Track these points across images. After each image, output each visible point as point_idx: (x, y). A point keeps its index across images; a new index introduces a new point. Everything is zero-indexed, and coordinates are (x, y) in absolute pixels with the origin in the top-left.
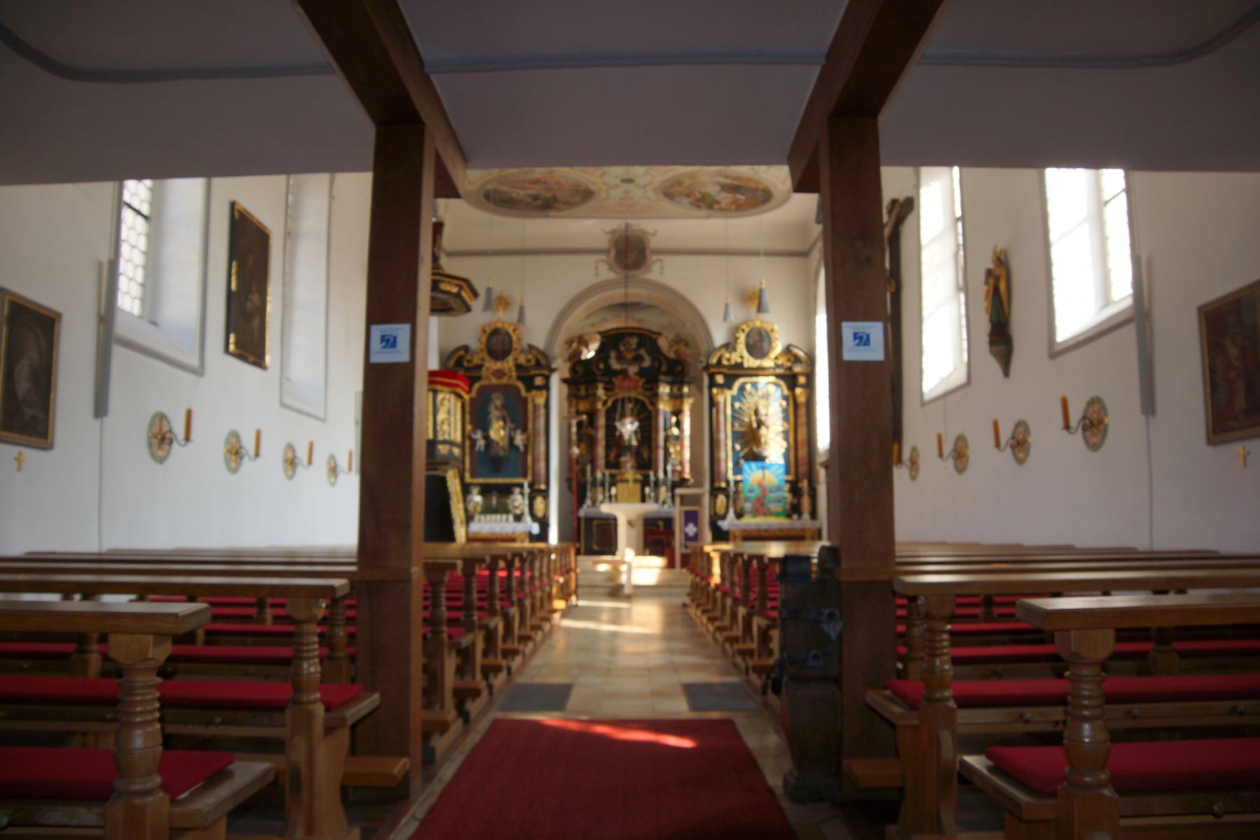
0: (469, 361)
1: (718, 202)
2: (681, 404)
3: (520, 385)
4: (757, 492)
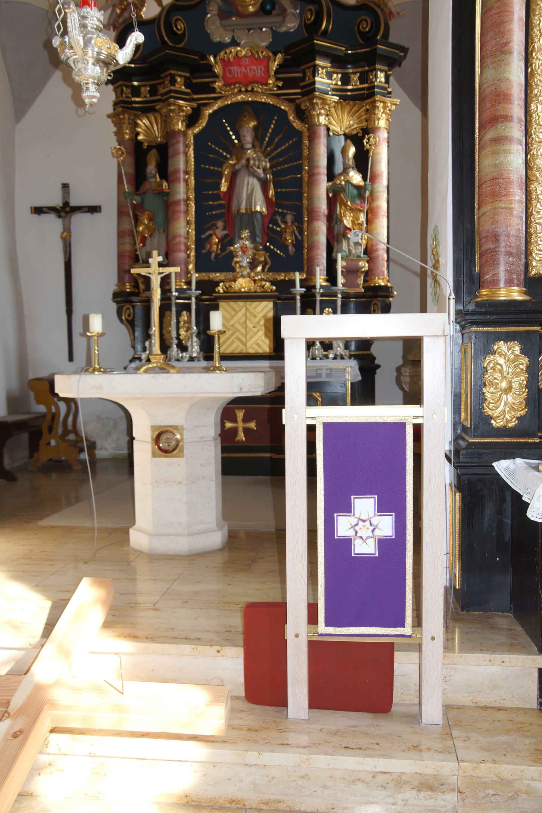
2: (371, 112)
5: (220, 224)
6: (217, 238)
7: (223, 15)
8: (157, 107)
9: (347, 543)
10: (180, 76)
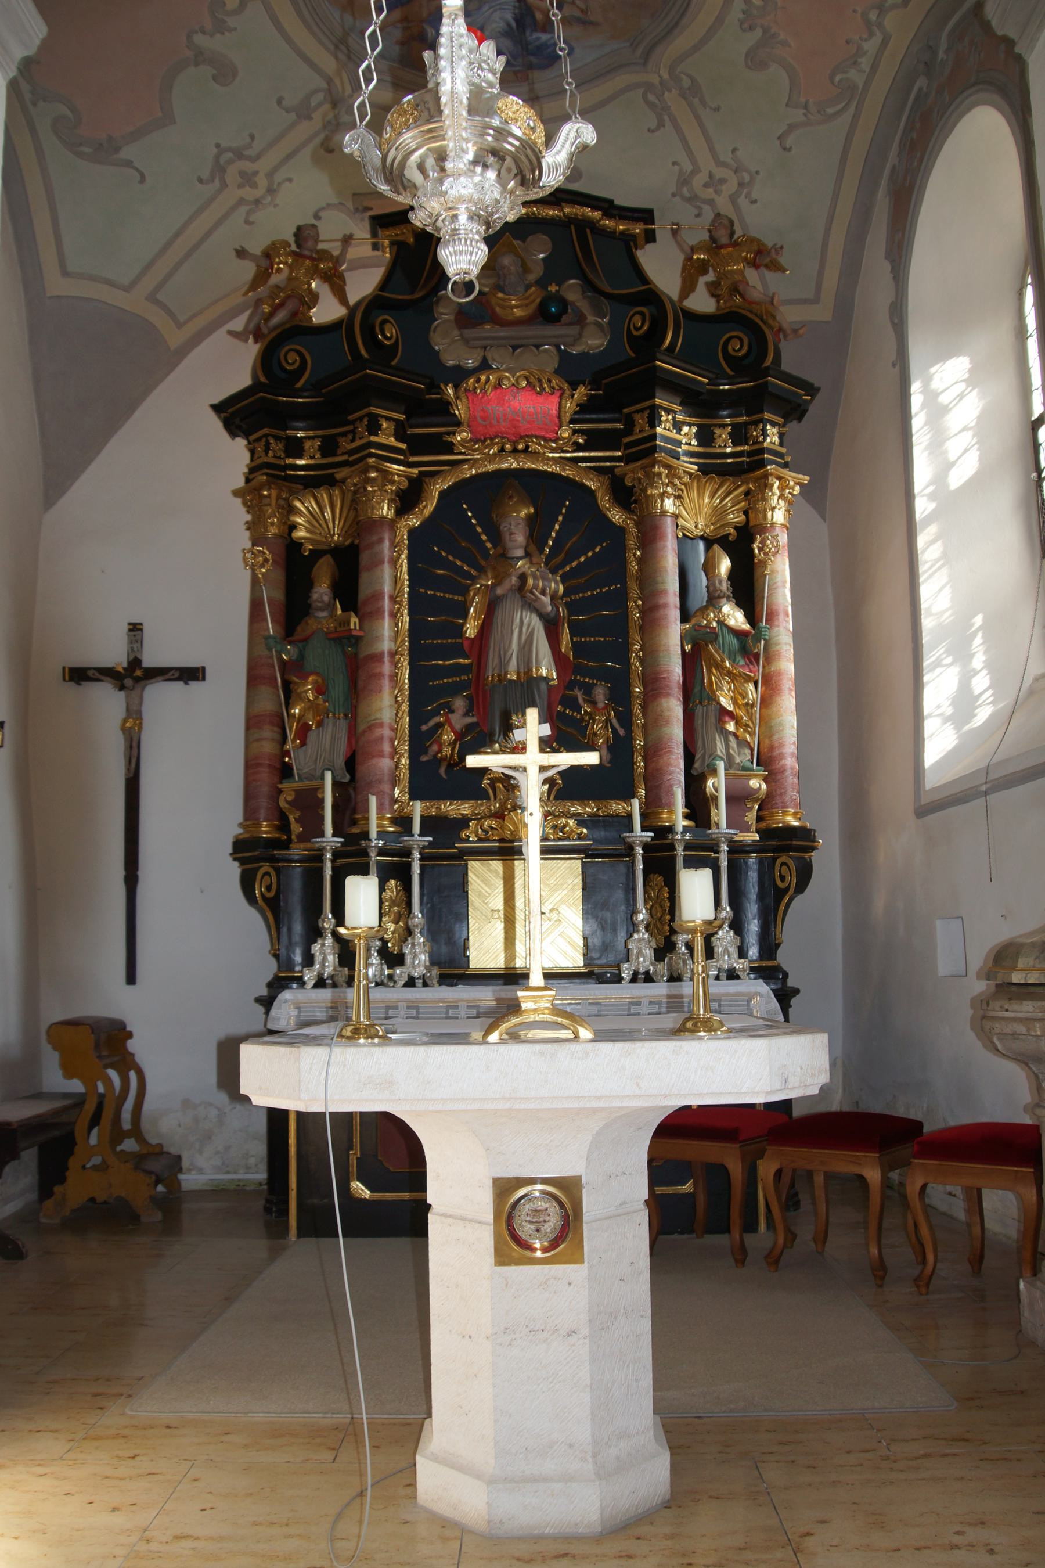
5: (459, 703)
6: (453, 730)
8: (338, 476)
10: (388, 419)
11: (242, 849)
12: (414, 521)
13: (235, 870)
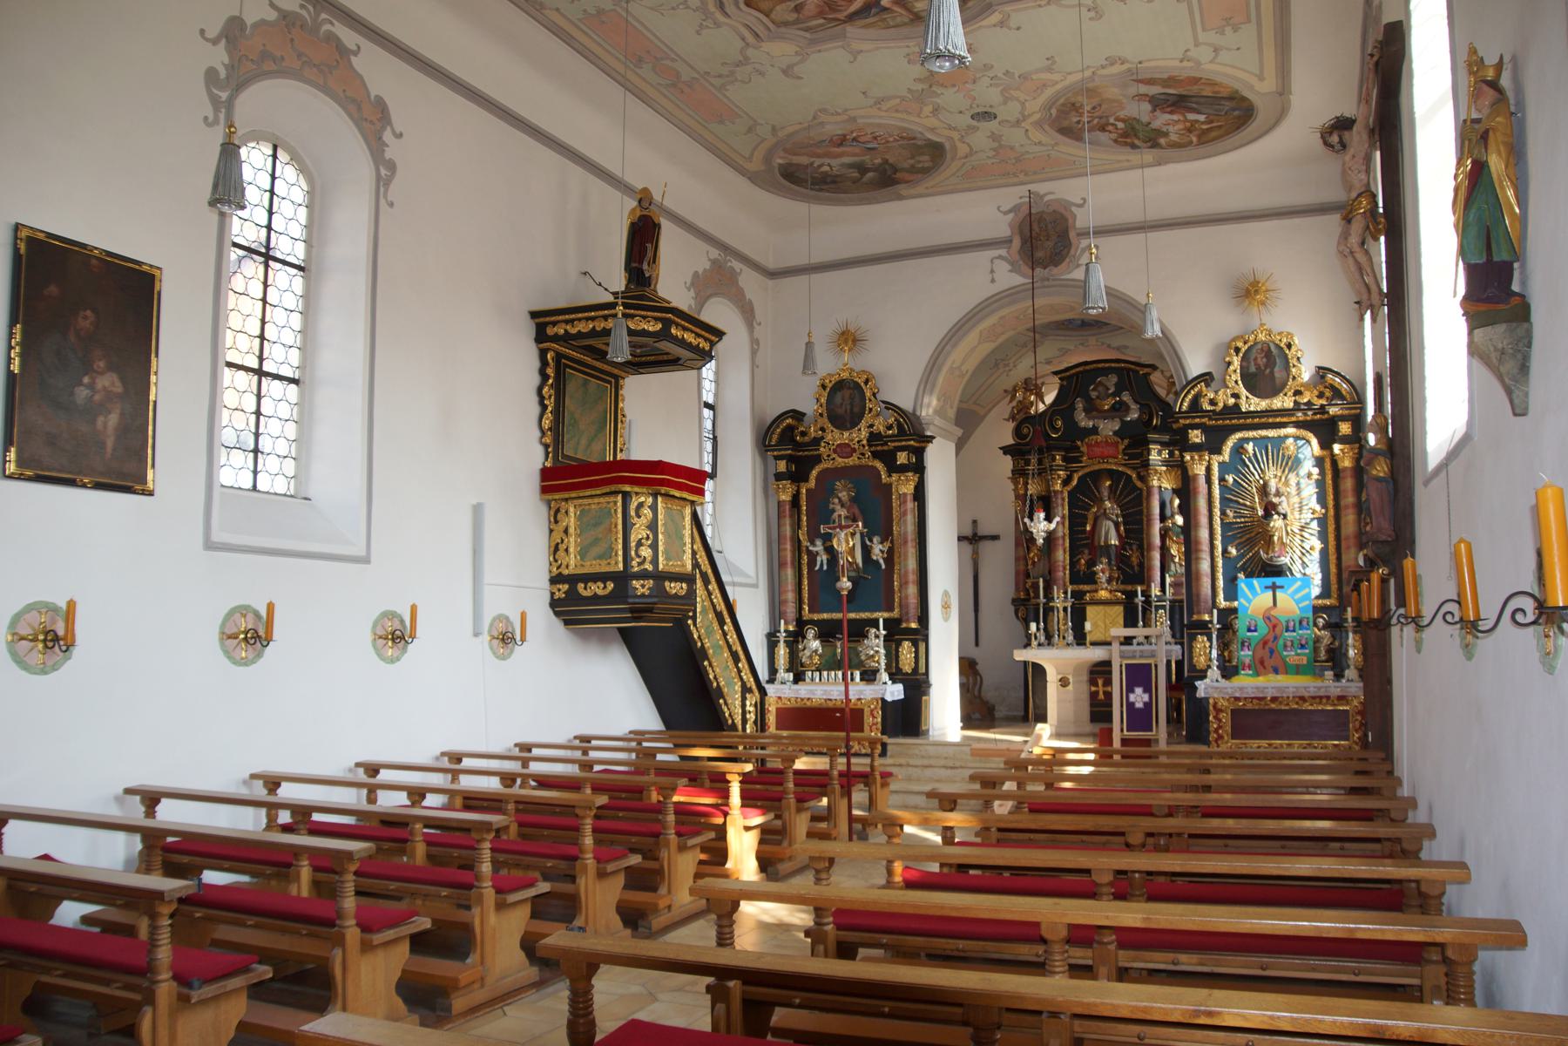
0: (803, 434)
1: (1166, 134)
3: (879, 465)
4: (1263, 629)
5: (1086, 551)
7: (1086, 410)
9: (1133, 704)
11: (1014, 601)
12: (1069, 488)
13: (1013, 608)
